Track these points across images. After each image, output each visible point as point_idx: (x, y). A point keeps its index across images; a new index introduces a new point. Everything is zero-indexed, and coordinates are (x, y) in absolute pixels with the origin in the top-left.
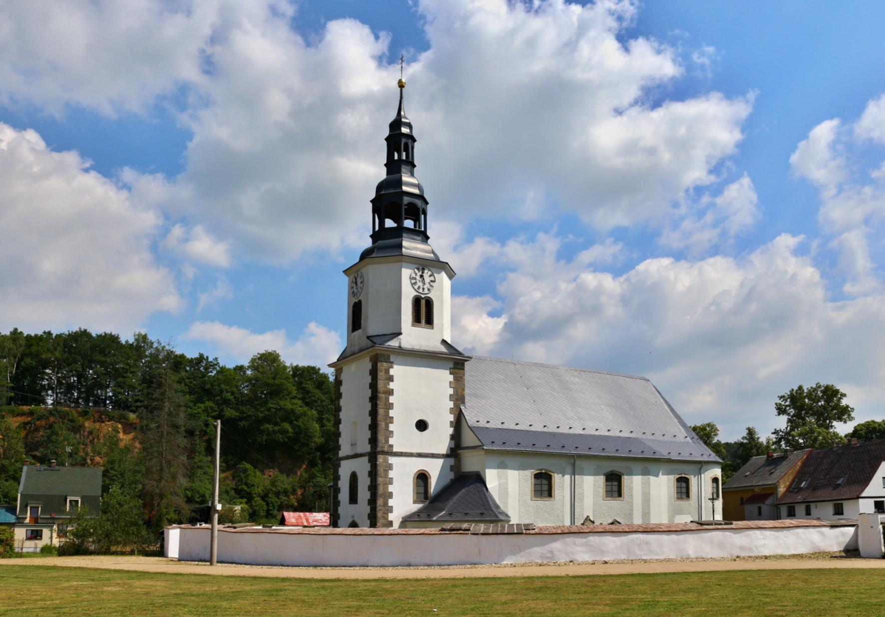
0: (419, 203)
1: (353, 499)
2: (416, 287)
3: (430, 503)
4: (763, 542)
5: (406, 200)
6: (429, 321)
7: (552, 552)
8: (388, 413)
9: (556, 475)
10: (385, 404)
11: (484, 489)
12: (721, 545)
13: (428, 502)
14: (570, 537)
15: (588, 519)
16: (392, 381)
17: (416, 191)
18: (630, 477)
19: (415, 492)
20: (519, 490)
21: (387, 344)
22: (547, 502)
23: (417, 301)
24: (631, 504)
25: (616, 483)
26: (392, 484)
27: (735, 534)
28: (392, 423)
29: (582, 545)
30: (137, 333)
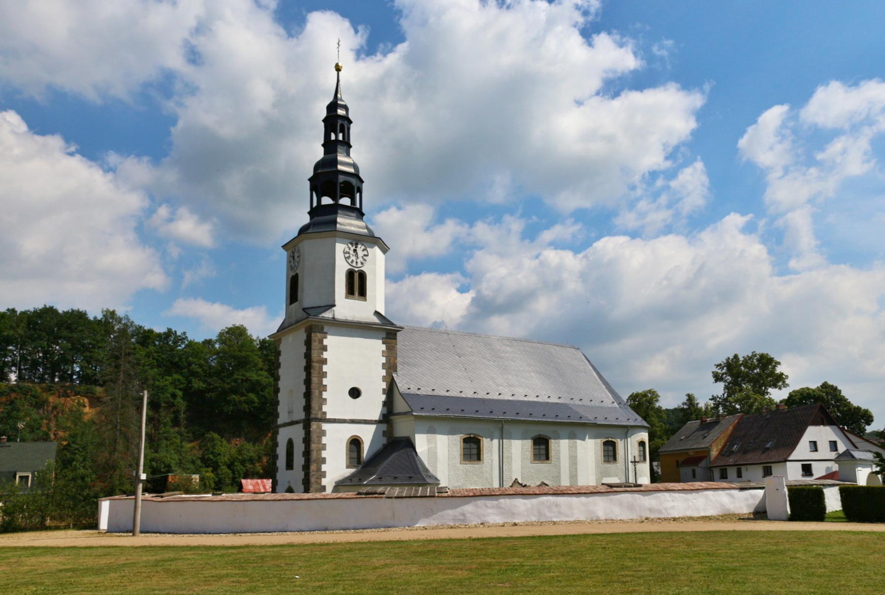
0: (354, 181)
1: (290, 465)
2: (350, 261)
3: (362, 468)
4: (671, 504)
5: (341, 178)
6: (363, 293)
7: (464, 515)
8: (322, 381)
9: (484, 439)
10: (319, 373)
11: (414, 453)
12: (631, 507)
13: (360, 467)
14: (481, 500)
15: (516, 481)
17: (352, 170)
18: (557, 441)
19: (348, 456)
20: (449, 454)
21: (321, 316)
22: (476, 466)
23: (350, 274)
24: (558, 467)
25: (543, 447)
26: (325, 450)
27: (644, 496)
28: (326, 391)
29: (493, 507)
30: (105, 310)
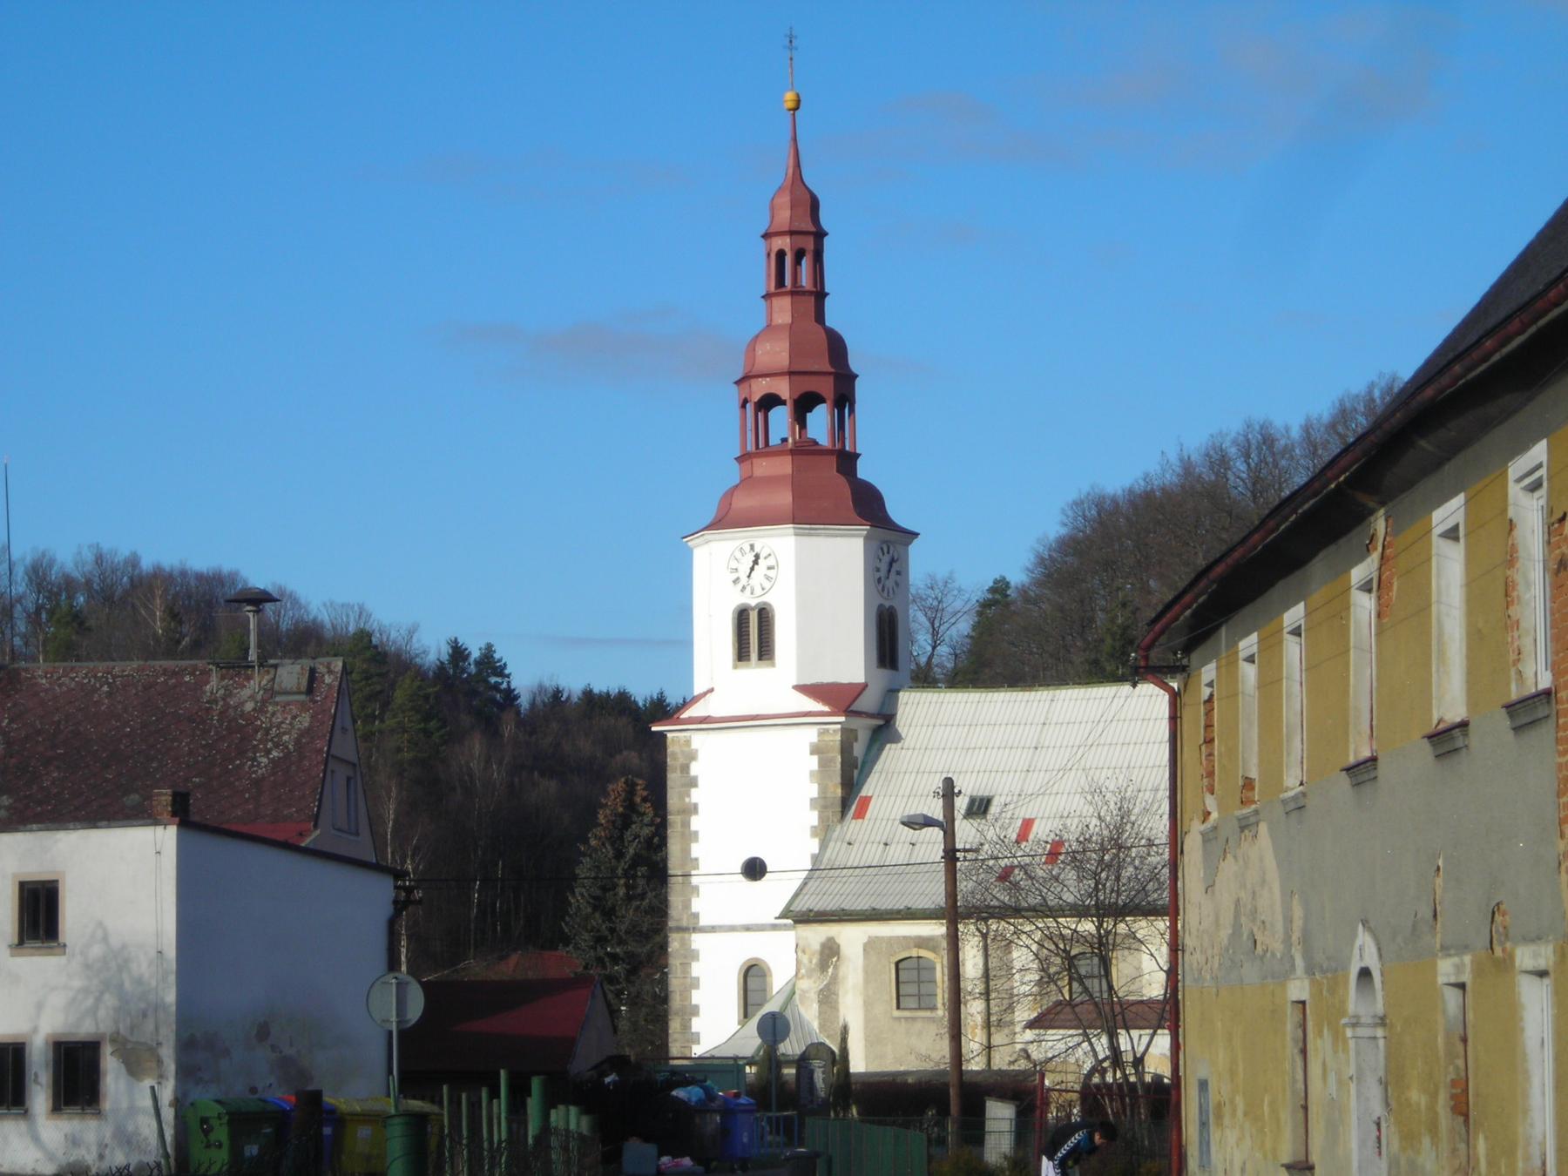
6: (766, 651)
16: (695, 785)
